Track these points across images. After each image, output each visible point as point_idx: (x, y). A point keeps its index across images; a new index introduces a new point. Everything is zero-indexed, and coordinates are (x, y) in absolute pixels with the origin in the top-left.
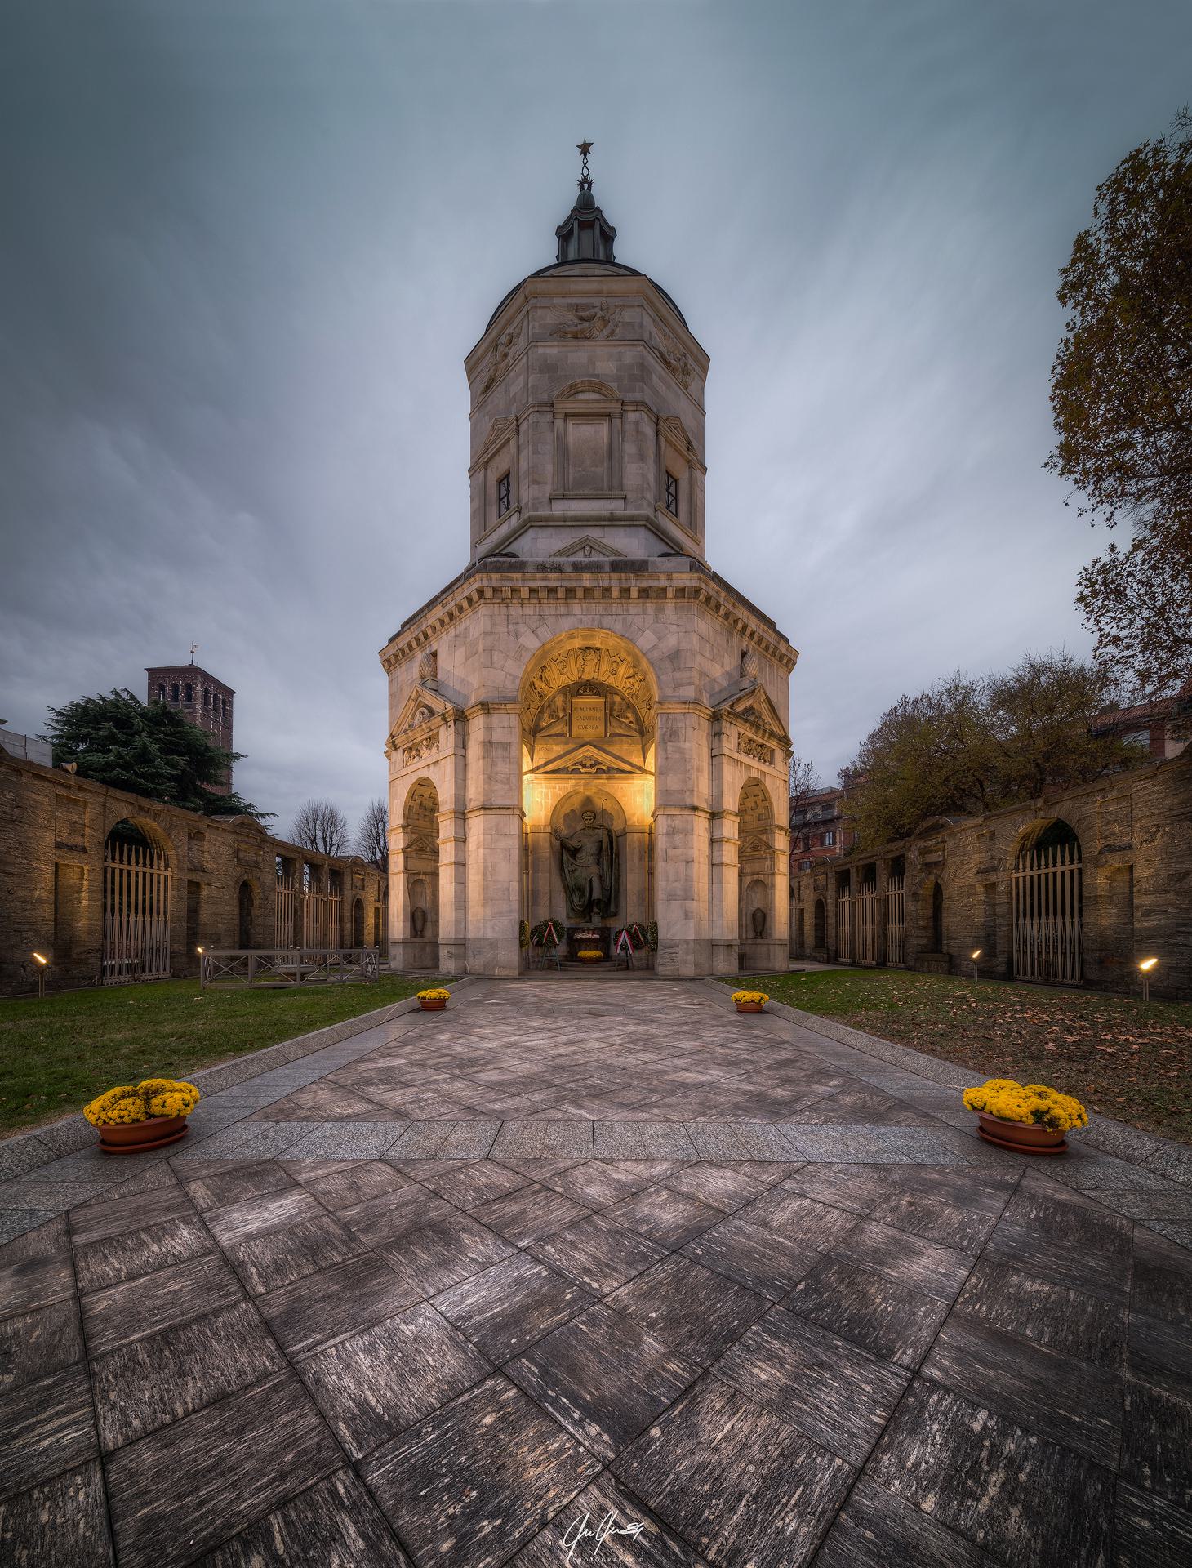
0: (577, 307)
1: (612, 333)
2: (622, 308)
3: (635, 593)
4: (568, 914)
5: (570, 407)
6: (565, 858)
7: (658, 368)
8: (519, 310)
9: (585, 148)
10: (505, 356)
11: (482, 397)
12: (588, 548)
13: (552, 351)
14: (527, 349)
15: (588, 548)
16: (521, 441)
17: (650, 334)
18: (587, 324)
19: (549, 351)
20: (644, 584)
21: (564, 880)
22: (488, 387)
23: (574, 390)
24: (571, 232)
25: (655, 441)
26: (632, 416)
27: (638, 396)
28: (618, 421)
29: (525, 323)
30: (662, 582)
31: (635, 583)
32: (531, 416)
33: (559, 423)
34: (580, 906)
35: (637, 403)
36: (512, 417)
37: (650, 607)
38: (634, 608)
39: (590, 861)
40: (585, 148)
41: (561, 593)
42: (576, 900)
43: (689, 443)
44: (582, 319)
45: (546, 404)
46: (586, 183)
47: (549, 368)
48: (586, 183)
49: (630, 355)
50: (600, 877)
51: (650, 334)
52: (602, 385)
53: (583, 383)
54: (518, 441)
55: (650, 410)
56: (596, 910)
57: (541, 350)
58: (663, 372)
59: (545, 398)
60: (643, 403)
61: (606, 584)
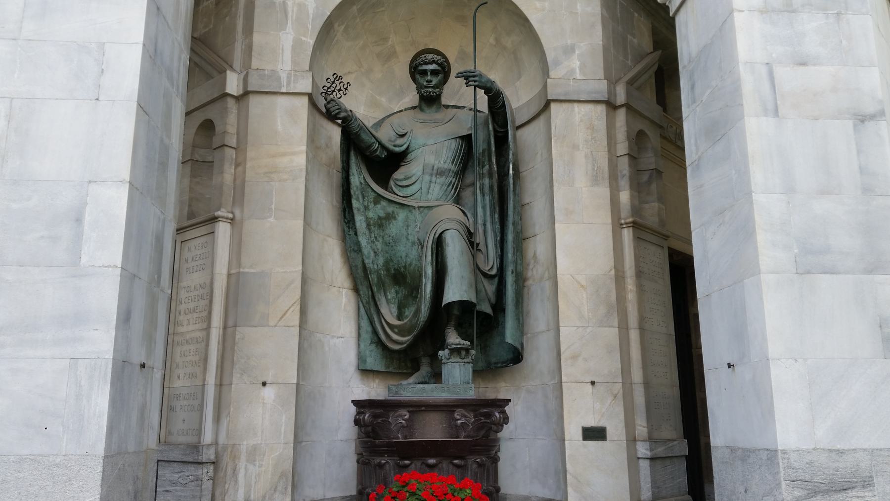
4: (361, 358)
34: (401, 331)
42: (389, 313)
56: (453, 338)
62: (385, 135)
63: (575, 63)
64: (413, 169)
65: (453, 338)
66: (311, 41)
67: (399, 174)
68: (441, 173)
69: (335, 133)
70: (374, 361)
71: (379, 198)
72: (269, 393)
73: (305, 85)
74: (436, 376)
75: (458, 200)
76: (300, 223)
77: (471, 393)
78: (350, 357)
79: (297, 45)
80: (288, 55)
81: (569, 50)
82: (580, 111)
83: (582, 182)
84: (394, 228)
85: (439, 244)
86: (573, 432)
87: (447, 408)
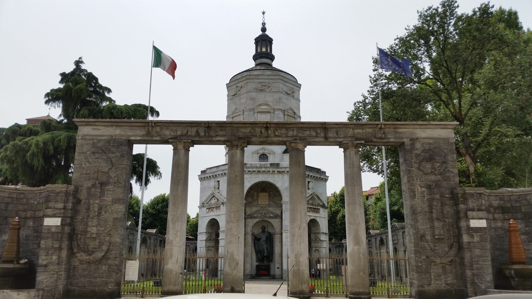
0: (261, 83)
1: (271, 90)
2: (274, 83)
3: (276, 172)
4: (256, 260)
5: (259, 110)
6: (256, 242)
7: (285, 96)
8: (244, 80)
9: (264, 13)
10: (240, 90)
11: (232, 97)
12: (264, 150)
13: (254, 94)
14: (247, 93)
15: (264, 150)
16: (244, 117)
17: (282, 88)
18: (264, 88)
19: (253, 94)
20: (279, 170)
21: (255, 249)
22: (233, 96)
23: (260, 105)
24: (259, 41)
25: (283, 117)
26: (277, 112)
27: (278, 107)
28: (273, 114)
29: (246, 85)
30: (284, 170)
31: (276, 170)
32: (247, 112)
33: (256, 114)
34: (260, 258)
35: (278, 109)
36: (242, 110)
37: (280, 176)
38: (276, 176)
39: (264, 243)
40: (264, 13)
41: (257, 172)
43: (295, 113)
44: (262, 86)
45: (252, 109)
46: (264, 24)
47: (253, 99)
48: (264, 24)
49: (277, 96)
50: (267, 249)
51: (282, 88)
52: (268, 104)
53: (262, 104)
54: (243, 116)
55: (282, 110)
56: (265, 259)
57: (250, 94)
58: (286, 97)
59: (251, 107)
60: (280, 109)
61: (268, 170)
62: (258, 237)
63: (278, 230)
64: (262, 240)
65: (265, 259)
66: (251, 228)
67: (260, 241)
68: (264, 241)
69: (254, 237)
70: (257, 260)
71: (258, 244)
72: (249, 264)
73: (251, 233)
74: (263, 262)
75: (266, 244)
76: (251, 248)
77: (267, 264)
78: (255, 260)
79: (250, 229)
80: (249, 230)
81: (277, 228)
82: (278, 235)
83: (278, 243)
84: (260, 247)
85: (264, 249)
86: (276, 268)
87: (265, 265)
